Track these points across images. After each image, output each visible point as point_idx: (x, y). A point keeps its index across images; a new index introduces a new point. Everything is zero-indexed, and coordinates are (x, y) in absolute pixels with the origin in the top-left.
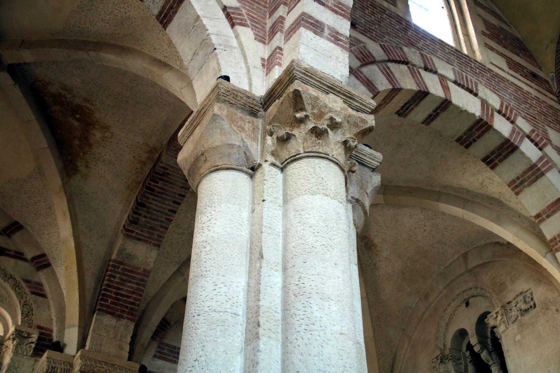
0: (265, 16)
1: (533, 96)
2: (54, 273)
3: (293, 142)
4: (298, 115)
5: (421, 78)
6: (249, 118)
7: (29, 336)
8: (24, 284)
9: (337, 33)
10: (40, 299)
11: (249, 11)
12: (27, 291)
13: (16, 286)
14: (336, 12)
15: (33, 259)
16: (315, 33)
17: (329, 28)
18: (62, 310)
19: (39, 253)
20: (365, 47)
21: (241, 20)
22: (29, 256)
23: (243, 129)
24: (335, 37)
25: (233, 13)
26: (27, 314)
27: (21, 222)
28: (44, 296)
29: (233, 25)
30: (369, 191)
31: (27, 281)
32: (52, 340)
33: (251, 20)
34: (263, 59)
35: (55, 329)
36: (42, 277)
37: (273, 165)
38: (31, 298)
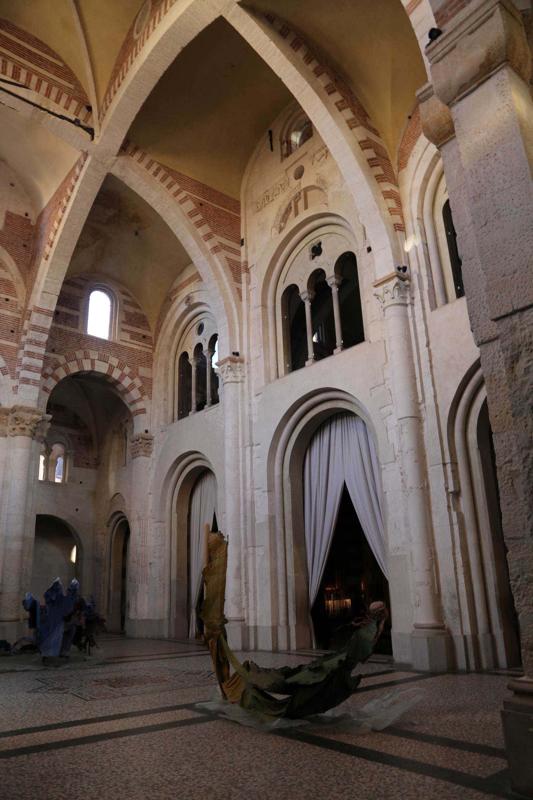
0: (15, 365)
1: (139, 351)
3: (16, 430)
4: (17, 422)
5: (82, 363)
6: (5, 417)
9: (35, 381)
11: (9, 366)
14: (36, 372)
16: (27, 384)
17: (33, 380)
20: (57, 361)
21: (6, 372)
23: (3, 423)
24: (35, 383)
25: (3, 370)
29: (3, 375)
30: (45, 431)
33: (10, 370)
34: (13, 387)
37: (11, 436)
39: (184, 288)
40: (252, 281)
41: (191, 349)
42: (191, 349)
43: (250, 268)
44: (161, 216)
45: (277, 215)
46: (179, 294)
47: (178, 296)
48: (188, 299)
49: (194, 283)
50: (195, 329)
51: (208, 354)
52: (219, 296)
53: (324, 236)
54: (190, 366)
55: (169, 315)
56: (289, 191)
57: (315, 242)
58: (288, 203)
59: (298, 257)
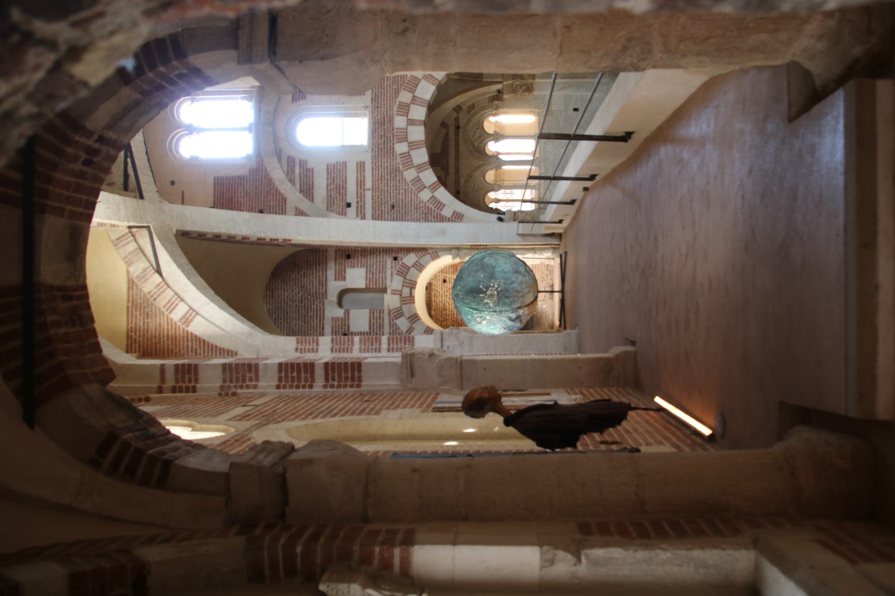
2: (462, 103)
7: (496, 105)
8: (471, 113)
10: (475, 105)
12: (473, 111)
13: (473, 116)
15: (457, 112)
18: (480, 95)
19: (454, 111)
22: (456, 115)
26: (484, 108)
27: (440, 123)
28: (473, 104)
31: (469, 113)
32: (494, 96)
35: (488, 96)
36: (465, 108)
38: (476, 109)
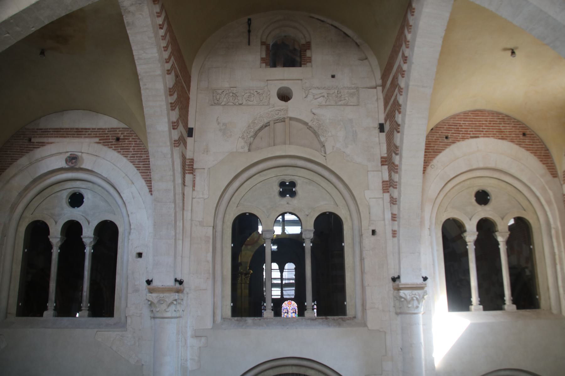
39: (65, 137)
40: (197, 187)
41: (56, 222)
42: (56, 222)
43: (195, 169)
44: (139, 77)
45: (249, 126)
46: (51, 140)
47: (48, 143)
48: (73, 159)
49: (87, 140)
50: (65, 195)
51: (91, 242)
52: (170, 202)
53: (302, 179)
54: (49, 246)
55: (23, 161)
56: (270, 110)
57: (288, 179)
58: (266, 121)
59: (261, 183)
